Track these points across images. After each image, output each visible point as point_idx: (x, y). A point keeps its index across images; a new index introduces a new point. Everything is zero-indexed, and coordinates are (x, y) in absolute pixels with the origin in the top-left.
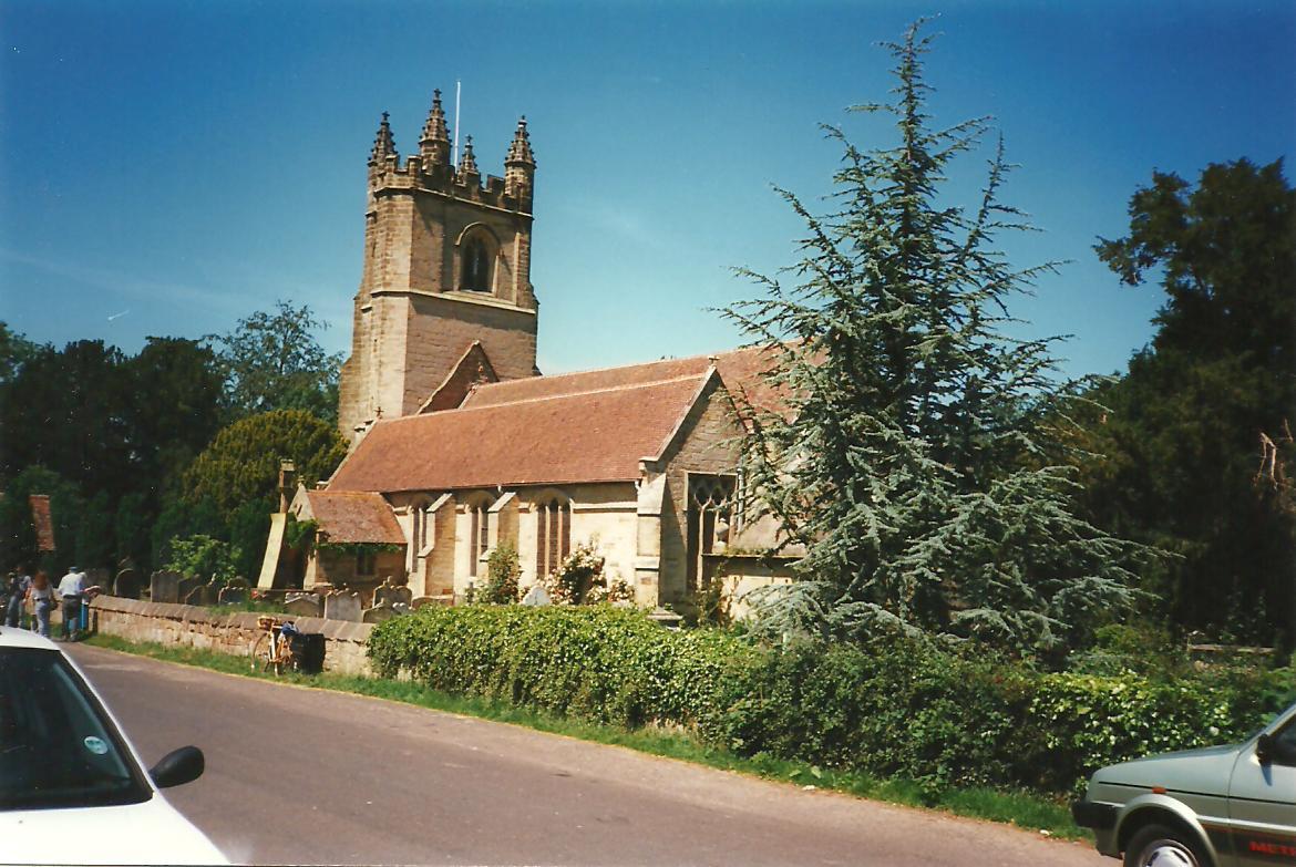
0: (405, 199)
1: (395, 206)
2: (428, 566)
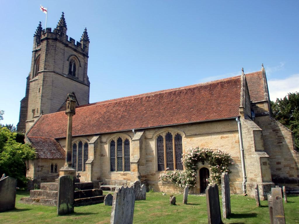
0: (52, 42)
1: (49, 43)
2: (92, 168)
